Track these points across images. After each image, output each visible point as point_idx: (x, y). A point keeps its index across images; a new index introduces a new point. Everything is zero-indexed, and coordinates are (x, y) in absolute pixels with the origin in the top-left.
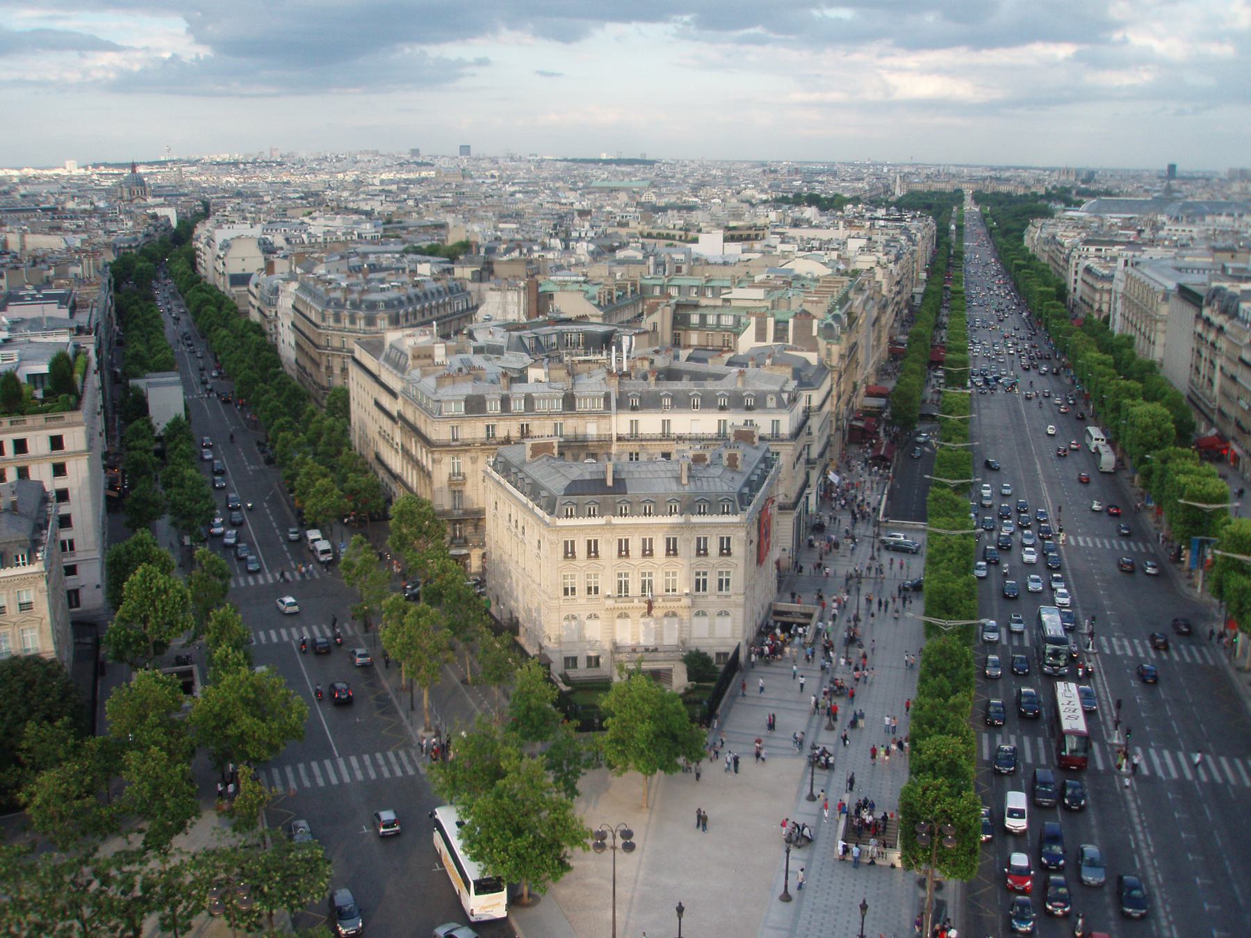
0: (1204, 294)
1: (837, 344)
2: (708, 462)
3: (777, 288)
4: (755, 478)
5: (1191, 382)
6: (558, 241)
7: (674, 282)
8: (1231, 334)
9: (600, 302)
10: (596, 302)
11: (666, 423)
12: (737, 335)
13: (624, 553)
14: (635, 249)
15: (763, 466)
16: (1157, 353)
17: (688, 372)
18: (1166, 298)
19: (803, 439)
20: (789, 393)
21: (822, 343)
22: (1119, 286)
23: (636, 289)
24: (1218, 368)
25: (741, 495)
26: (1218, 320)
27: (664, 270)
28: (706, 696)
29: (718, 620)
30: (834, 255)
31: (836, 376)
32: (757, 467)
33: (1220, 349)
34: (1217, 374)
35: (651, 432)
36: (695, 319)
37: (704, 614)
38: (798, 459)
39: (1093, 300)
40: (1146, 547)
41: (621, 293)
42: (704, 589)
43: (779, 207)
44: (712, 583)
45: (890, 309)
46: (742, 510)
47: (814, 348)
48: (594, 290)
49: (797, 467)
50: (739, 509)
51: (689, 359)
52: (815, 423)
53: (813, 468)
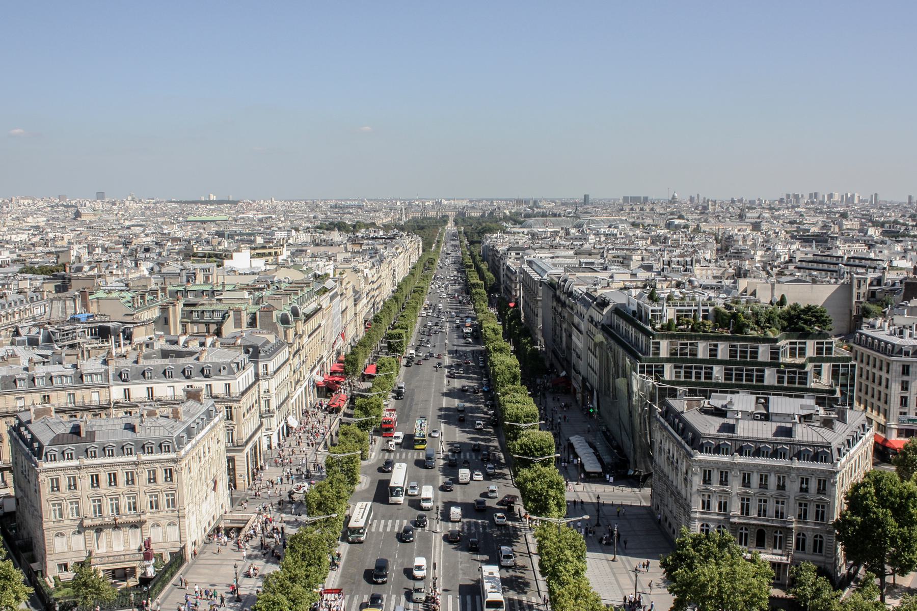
2: (158, 416)
4: (194, 425)
5: (554, 340)
6: (129, 261)
8: (569, 306)
10: (130, 304)
11: (150, 390)
13: (113, 484)
18: (541, 286)
20: (238, 364)
21: (281, 328)
23: (166, 294)
29: (168, 528)
32: (199, 418)
34: (564, 335)
39: (511, 287)
45: (364, 301)
48: (128, 296)
49: (247, 416)
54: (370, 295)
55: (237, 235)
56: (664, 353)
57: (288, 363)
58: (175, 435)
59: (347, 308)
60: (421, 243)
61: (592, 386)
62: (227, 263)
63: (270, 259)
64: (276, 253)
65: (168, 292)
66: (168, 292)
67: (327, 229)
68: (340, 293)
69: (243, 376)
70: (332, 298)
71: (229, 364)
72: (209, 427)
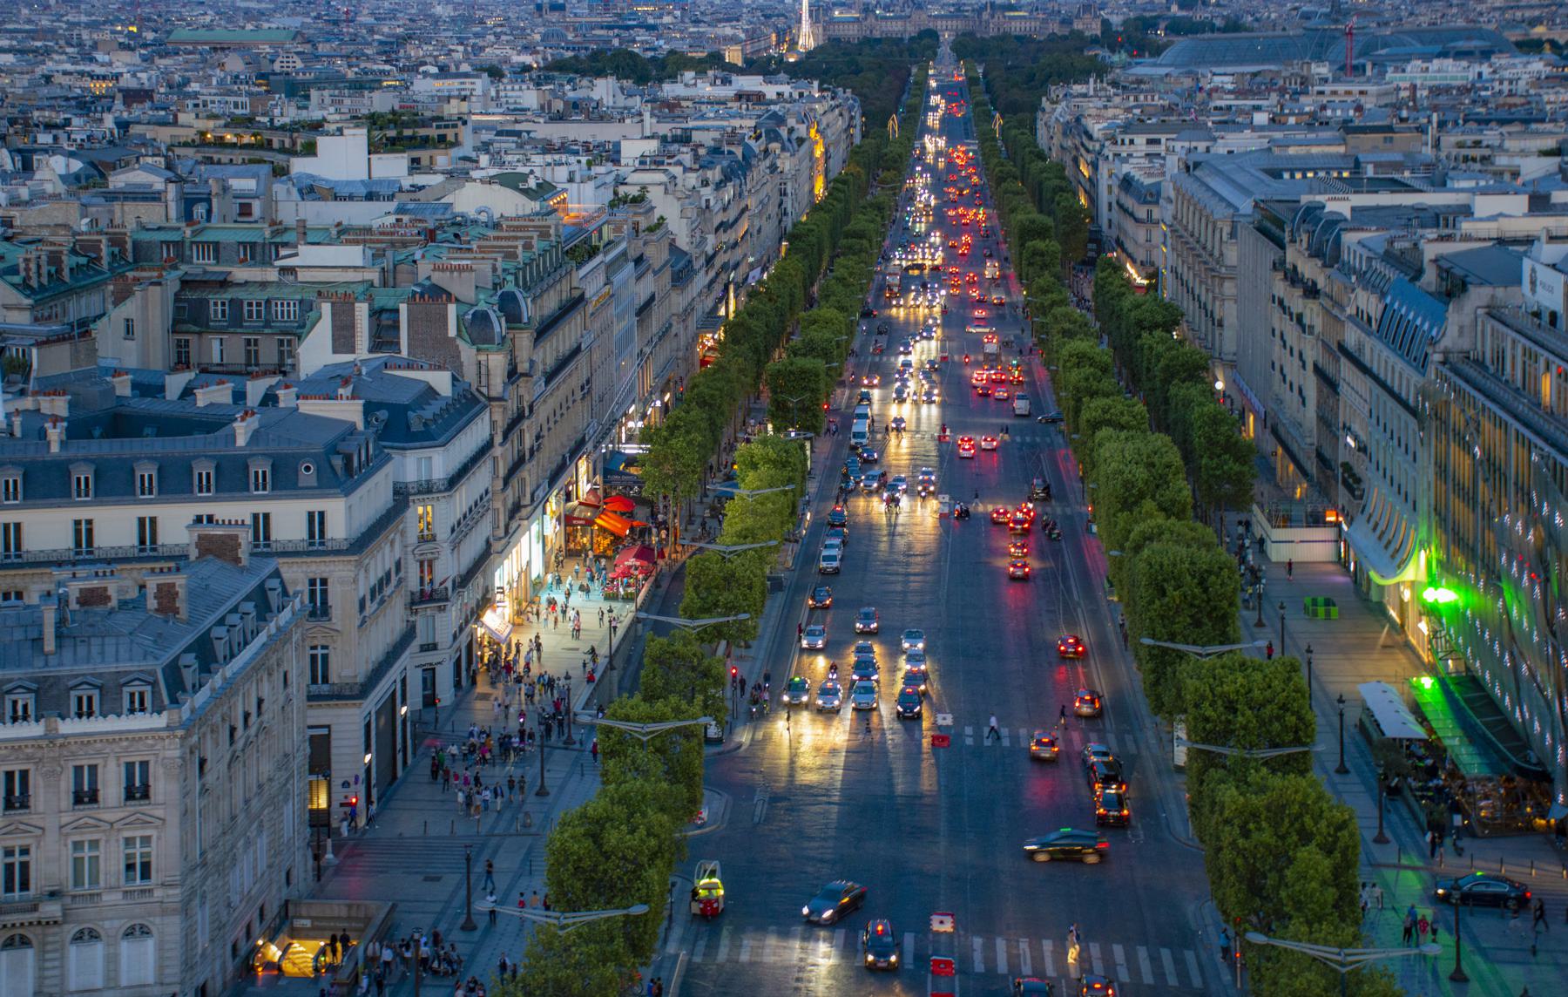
1: (498, 351)
7: (208, 236)
9: (26, 279)
10: (17, 279)
14: (151, 169)
15: (249, 607)
21: (467, 353)
23: (123, 251)
25: (174, 675)
27: (209, 212)
32: (234, 610)
35: (48, 547)
41: (83, 260)
43: (549, 80)
45: (701, 280)
46: (175, 701)
47: (448, 359)
49: (370, 607)
50: (166, 701)
53: (442, 609)
54: (718, 262)
58: (167, 657)
59: (652, 298)
62: (299, 166)
63: (424, 155)
64: (442, 138)
65: (129, 246)
66: (129, 246)
67: (583, 74)
68: (633, 254)
70: (612, 268)
72: (262, 638)
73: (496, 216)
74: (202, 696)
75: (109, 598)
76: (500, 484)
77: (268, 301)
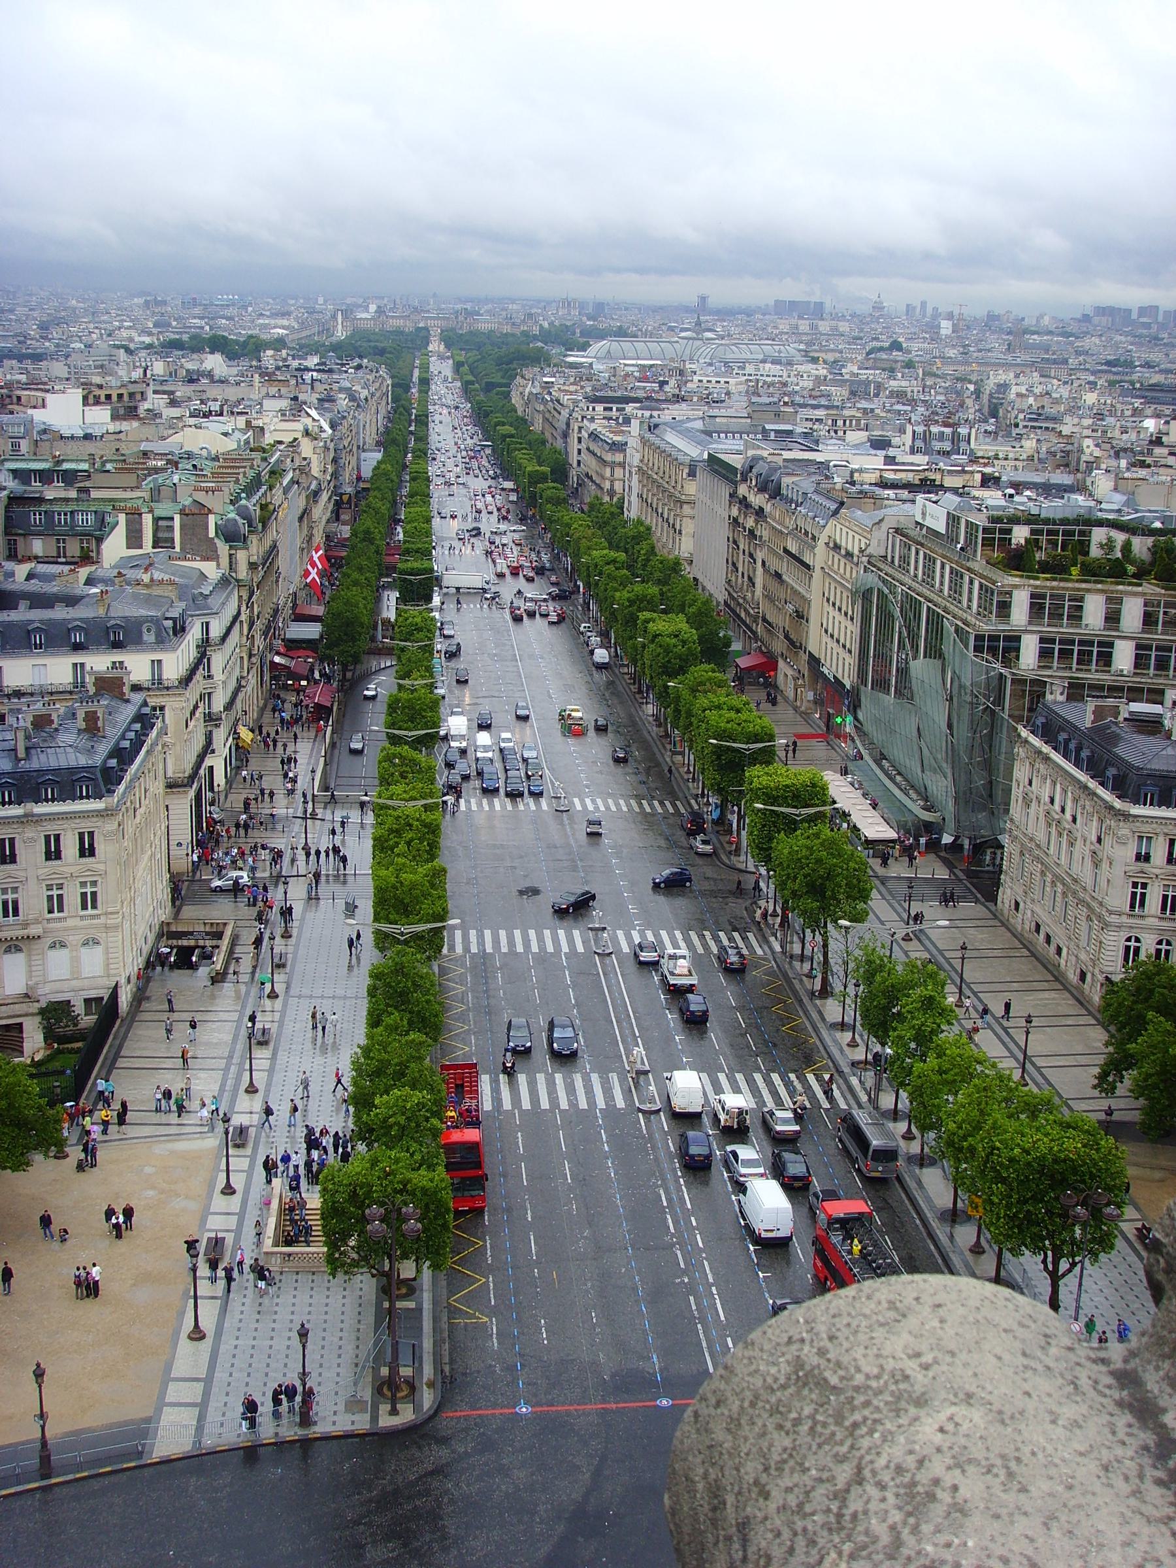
0: (739, 466)
3: (157, 470)
4: (126, 744)
5: (729, 582)
12: (100, 540)
15: (138, 726)
16: (686, 547)
17: (26, 595)
18: (692, 474)
19: (199, 684)
20: (174, 620)
21: (223, 548)
22: (634, 457)
24: (759, 563)
26: (756, 500)
28: (70, 1063)
29: (84, 950)
30: (241, 421)
31: (245, 597)
32: (128, 729)
33: (761, 537)
36: (36, 519)
37: (63, 945)
38: (193, 713)
39: (603, 478)
40: (674, 806)
42: (61, 910)
44: (72, 898)
45: (325, 496)
47: (210, 555)
49: (191, 724)
51: (30, 576)
52: (218, 660)
53: (217, 726)
55: (10, 357)
56: (1020, 613)
57: (238, 624)
60: (390, 382)
61: (835, 677)
69: (183, 646)
70: (286, 491)
71: (156, 621)
73: (213, 452)
74: (122, 787)
75: (52, 722)
76: (245, 638)
77: (72, 512)
